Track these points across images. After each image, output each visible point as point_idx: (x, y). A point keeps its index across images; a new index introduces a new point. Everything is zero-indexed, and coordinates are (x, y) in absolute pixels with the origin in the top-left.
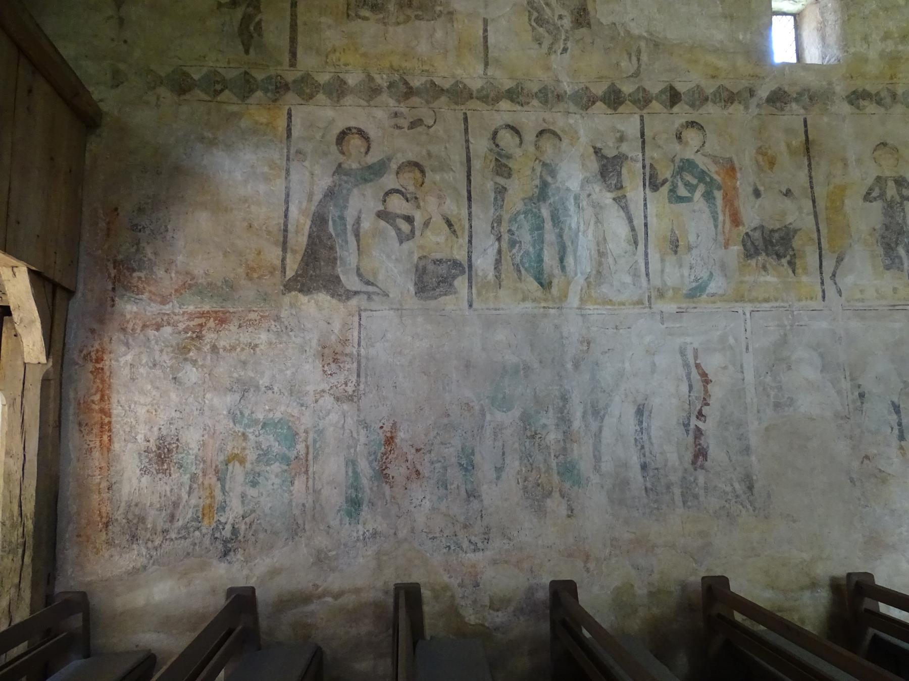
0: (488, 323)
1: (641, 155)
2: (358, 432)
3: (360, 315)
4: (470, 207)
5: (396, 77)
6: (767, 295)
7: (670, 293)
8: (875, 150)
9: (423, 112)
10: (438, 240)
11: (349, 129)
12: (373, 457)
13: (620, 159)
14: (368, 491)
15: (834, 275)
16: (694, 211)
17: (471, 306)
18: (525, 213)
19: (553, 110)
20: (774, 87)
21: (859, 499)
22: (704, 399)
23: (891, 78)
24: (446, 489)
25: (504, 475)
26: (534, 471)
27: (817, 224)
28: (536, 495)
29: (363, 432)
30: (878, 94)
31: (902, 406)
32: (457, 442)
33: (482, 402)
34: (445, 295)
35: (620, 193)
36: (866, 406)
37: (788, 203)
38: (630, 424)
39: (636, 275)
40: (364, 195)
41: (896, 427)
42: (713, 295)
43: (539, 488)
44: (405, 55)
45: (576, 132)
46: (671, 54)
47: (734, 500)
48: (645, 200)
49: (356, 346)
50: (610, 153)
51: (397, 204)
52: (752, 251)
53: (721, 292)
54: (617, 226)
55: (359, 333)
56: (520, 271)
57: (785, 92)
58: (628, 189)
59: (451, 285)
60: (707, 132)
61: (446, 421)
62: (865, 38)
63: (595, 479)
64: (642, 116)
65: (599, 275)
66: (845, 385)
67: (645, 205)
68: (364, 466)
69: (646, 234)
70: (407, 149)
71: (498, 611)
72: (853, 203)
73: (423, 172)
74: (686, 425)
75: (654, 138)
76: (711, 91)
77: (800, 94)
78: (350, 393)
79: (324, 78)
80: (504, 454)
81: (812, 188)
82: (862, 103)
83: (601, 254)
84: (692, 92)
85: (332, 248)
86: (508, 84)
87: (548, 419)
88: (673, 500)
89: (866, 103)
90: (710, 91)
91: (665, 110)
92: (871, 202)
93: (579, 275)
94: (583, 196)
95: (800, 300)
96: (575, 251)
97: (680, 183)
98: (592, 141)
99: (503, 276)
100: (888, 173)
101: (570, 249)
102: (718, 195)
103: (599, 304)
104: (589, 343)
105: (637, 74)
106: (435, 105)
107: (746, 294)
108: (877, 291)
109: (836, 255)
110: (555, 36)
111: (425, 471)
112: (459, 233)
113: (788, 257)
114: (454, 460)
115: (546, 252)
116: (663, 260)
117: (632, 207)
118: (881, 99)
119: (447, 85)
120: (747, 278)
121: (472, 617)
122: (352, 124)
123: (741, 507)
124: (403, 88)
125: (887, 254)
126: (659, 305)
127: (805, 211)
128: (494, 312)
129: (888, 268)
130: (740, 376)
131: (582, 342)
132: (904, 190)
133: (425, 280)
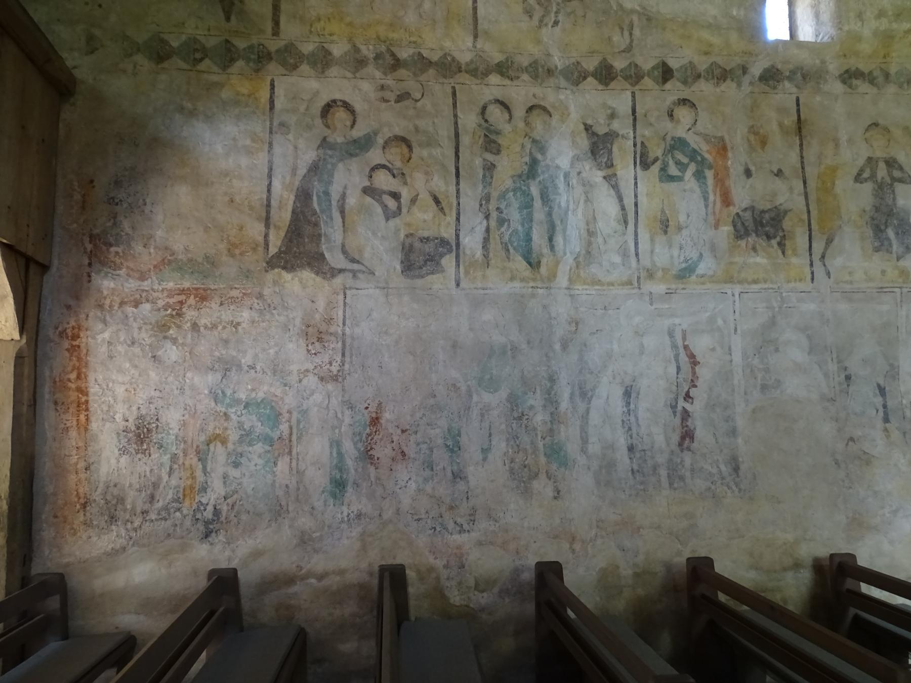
0: (474, 304)
1: (632, 132)
2: (342, 412)
3: (345, 294)
4: (458, 184)
5: (383, 48)
7: (660, 274)
8: (867, 130)
10: (426, 217)
11: (334, 101)
12: (358, 438)
13: (611, 136)
14: (353, 471)
15: (823, 257)
16: (685, 191)
17: (458, 285)
18: (515, 190)
19: (544, 85)
20: (766, 64)
21: (843, 481)
22: (692, 381)
23: (885, 57)
24: (432, 470)
25: (490, 456)
26: (521, 452)
27: (807, 205)
28: (523, 477)
29: (348, 412)
30: (871, 73)
32: (443, 423)
33: (469, 383)
34: (433, 273)
35: (610, 172)
36: (851, 389)
37: (779, 184)
38: (617, 406)
39: (625, 255)
40: (349, 170)
41: (881, 410)
42: (702, 276)
43: (526, 470)
44: (392, 26)
45: (567, 108)
46: (664, 29)
47: (720, 482)
48: (636, 179)
49: (341, 325)
50: (601, 130)
51: (383, 180)
53: (711, 273)
54: (607, 205)
55: (344, 312)
56: (508, 250)
57: (778, 70)
58: (619, 167)
59: (438, 263)
61: (432, 401)
62: (860, 16)
63: (582, 460)
64: (633, 94)
65: (588, 254)
66: (833, 367)
67: (636, 184)
68: (348, 447)
69: (636, 213)
70: (393, 122)
71: (483, 592)
72: (843, 184)
73: (410, 147)
74: (674, 407)
75: (645, 116)
76: (705, 67)
77: (793, 72)
78: (335, 373)
79: (308, 48)
80: (490, 435)
81: (803, 168)
82: (855, 82)
83: (591, 233)
84: (684, 68)
85: (316, 225)
86: (498, 57)
87: (535, 400)
88: (659, 481)
90: (702, 67)
91: (657, 87)
92: (861, 183)
93: (568, 254)
94: (573, 174)
95: (789, 282)
96: (564, 230)
97: (671, 162)
99: (491, 255)
100: (879, 154)
101: (559, 228)
102: (709, 174)
104: (577, 324)
105: (629, 49)
106: (423, 78)
107: (735, 275)
108: (866, 273)
109: (825, 237)
110: (546, 8)
111: (411, 451)
112: (446, 210)
113: (778, 239)
114: (440, 441)
115: (534, 231)
116: (652, 240)
117: (622, 184)
118: (874, 78)
119: (435, 58)
121: (458, 598)
122: (338, 96)
123: (726, 488)
124: (389, 60)
127: (796, 191)
128: (482, 292)
129: (877, 250)
131: (569, 324)
133: (411, 258)
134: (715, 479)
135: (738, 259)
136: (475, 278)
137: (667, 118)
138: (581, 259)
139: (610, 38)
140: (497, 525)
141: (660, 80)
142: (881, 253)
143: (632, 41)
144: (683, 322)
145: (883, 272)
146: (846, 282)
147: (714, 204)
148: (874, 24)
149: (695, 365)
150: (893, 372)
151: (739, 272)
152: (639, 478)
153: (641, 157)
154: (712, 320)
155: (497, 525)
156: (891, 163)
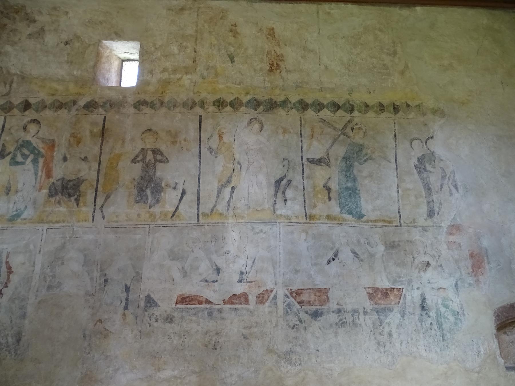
6: (58, 219)
8: (143, 133)
15: (102, 207)
22: (6, 283)
23: (162, 93)
27: (98, 176)
30: (152, 102)
31: (131, 288)
36: (106, 287)
37: (84, 165)
42: (25, 219)
46: (31, 83)
53: (30, 217)
57: (96, 102)
60: (42, 125)
66: (96, 274)
72: (124, 164)
76: (50, 102)
77: (105, 103)
81: (100, 156)
89: (144, 107)
91: (20, 114)
92: (135, 163)
95: (78, 222)
97: (19, 155)
100: (148, 146)
102: (41, 161)
109: (105, 195)
113: (76, 196)
120: (48, 209)
123: (7, 353)
125: (139, 193)
127: (93, 169)
129: (137, 202)
132: (158, 156)
134: (3, 347)
137: (22, 130)
141: (23, 110)
143: (10, 89)
145: (139, 215)
147: (41, 177)
148: (159, 76)
150: (138, 277)
151: (47, 216)
156: (156, 152)
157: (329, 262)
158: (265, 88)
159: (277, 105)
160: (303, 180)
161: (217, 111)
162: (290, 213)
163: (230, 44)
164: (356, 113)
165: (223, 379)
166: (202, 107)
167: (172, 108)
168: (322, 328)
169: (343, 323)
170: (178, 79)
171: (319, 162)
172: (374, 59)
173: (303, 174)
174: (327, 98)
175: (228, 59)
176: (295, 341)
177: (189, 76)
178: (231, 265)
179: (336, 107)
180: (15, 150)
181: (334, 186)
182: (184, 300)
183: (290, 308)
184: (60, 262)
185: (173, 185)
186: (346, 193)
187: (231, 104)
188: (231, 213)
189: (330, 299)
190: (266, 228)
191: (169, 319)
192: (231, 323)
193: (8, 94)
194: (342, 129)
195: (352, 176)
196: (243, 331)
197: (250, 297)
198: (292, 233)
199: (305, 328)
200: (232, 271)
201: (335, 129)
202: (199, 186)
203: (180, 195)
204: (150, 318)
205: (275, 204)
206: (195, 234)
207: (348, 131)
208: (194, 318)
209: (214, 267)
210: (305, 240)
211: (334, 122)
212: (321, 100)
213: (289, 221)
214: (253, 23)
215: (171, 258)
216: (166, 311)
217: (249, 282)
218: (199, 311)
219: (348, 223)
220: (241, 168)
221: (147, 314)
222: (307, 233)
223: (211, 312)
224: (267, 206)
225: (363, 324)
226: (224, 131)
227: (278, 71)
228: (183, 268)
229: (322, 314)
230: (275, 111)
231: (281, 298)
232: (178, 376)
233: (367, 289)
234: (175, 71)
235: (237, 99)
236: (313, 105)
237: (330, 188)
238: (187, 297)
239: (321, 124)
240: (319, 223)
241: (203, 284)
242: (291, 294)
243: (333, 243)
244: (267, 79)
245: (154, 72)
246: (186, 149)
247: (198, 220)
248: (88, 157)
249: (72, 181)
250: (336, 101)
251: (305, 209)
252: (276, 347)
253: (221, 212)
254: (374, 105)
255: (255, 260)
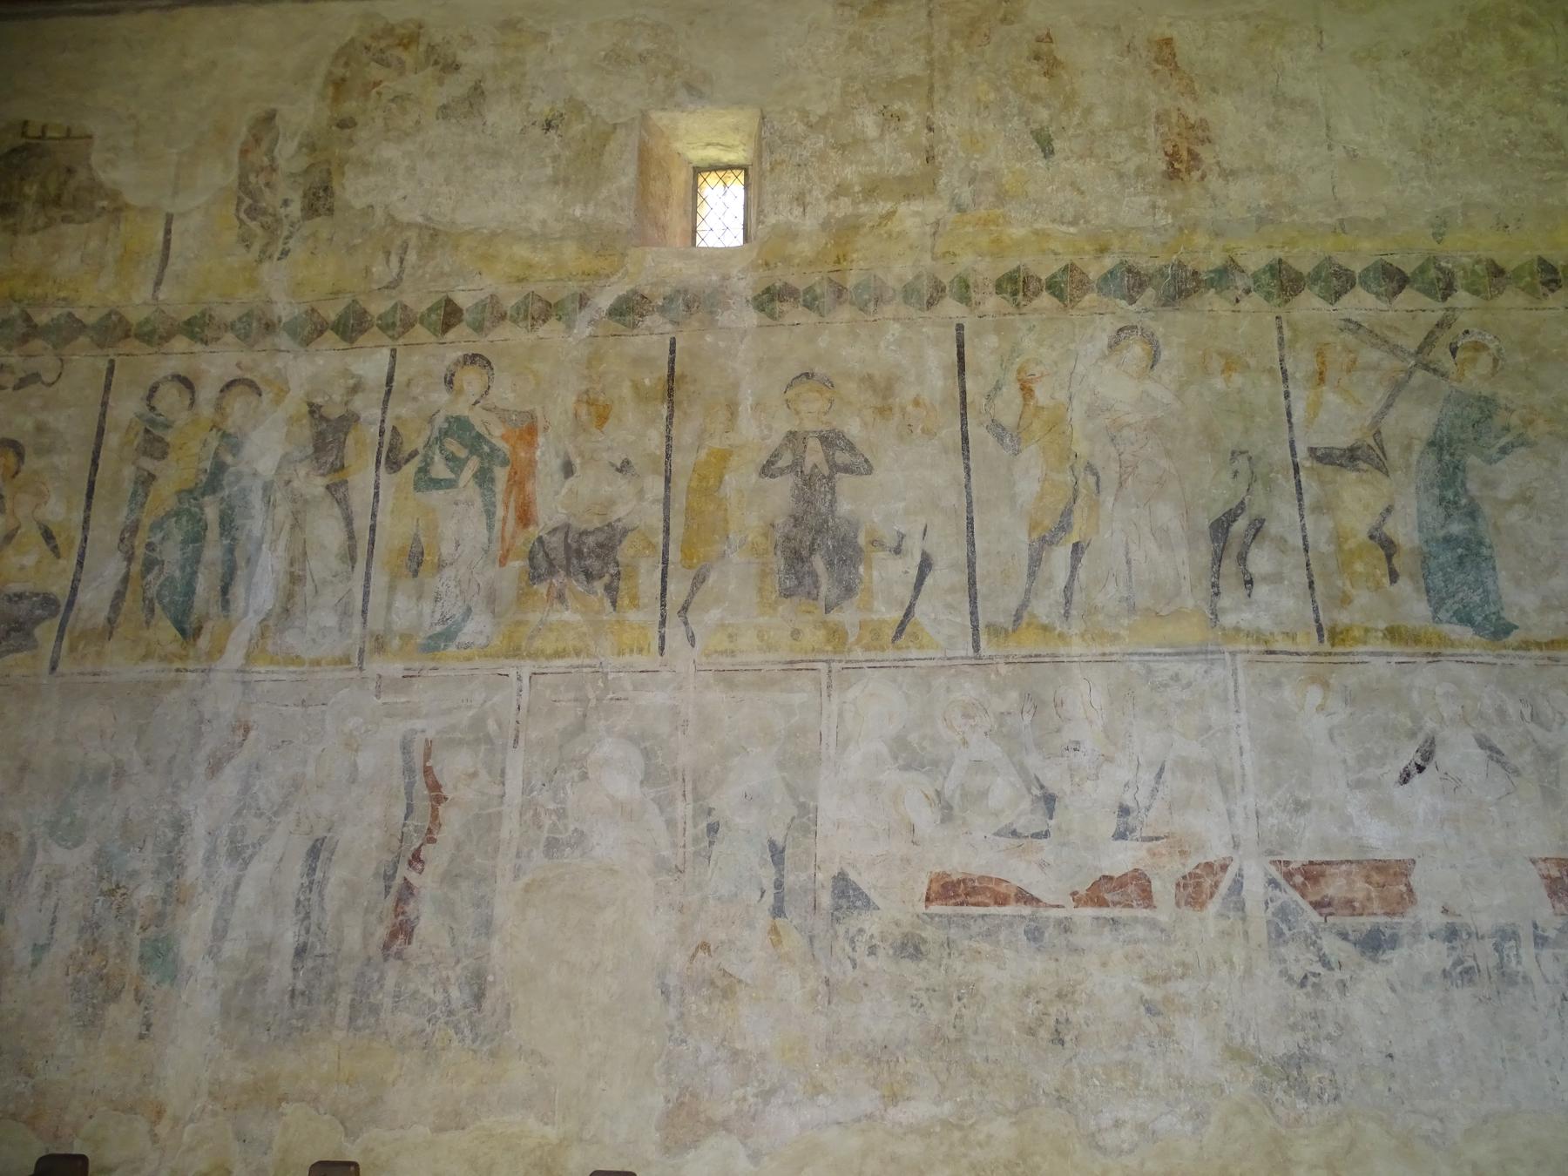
1: (379, 412)
4: (88, 507)
6: (561, 646)
7: (396, 642)
8: (790, 386)
9: (46, 362)
13: (349, 421)
15: (685, 608)
17: (53, 668)
21: (671, 1028)
22: (430, 831)
23: (838, 261)
27: (667, 520)
30: (810, 289)
34: (17, 650)
35: (336, 478)
36: (716, 849)
37: (623, 485)
39: (345, 614)
44: (34, 278)
45: (286, 382)
48: (377, 487)
50: (334, 412)
52: (544, 566)
53: (482, 641)
54: (327, 532)
56: (152, 611)
59: (29, 635)
63: (205, 969)
64: (394, 351)
65: (286, 610)
66: (683, 809)
67: (376, 495)
72: (739, 479)
73: (20, 456)
74: (388, 878)
75: (408, 385)
77: (669, 299)
80: (53, 923)
81: (668, 456)
84: (481, 307)
87: (143, 861)
88: (332, 1015)
89: (785, 307)
90: (509, 304)
91: (433, 339)
92: (773, 476)
93: (251, 614)
95: (620, 653)
96: (251, 575)
98: (307, 395)
99: (121, 619)
100: (809, 425)
101: (241, 573)
102: (501, 474)
103: (278, 663)
104: (247, 730)
108: (760, 637)
109: (692, 573)
112: (62, 549)
113: (607, 579)
116: (392, 588)
119: (91, 319)
123: (451, 1032)
124: (21, 328)
125: (790, 566)
126: (375, 666)
127: (649, 496)
129: (787, 594)
130: (497, 790)
132: (838, 454)
135: (534, 617)
136: (84, 656)
138: (271, 623)
139: (367, 270)
140: (31, 1082)
142: (795, 599)
144: (428, 727)
145: (796, 634)
146: (723, 653)
149: (439, 803)
150: (805, 819)
151: (531, 638)
152: (300, 1005)
153: (390, 450)
154: (478, 723)
155: (31, 1082)
156: (830, 440)
157: (1406, 778)
158: (1155, 230)
159: (1199, 282)
160: (1302, 517)
161: (1011, 310)
162: (1265, 623)
163: (1036, 98)
164: (1462, 298)
165: (1093, 1135)
166: (964, 298)
167: (871, 306)
168: (1398, 987)
169: (1468, 971)
170: (881, 217)
171: (1351, 457)
172: (1513, 119)
173: (1300, 500)
174: (1361, 254)
175: (1034, 145)
176: (1313, 1023)
177: (916, 206)
178: (1089, 785)
179: (1393, 279)
180: (428, 445)
181: (1404, 531)
182: (949, 890)
183: (1287, 921)
184: (575, 773)
185: (891, 542)
186: (1447, 557)
187: (1053, 287)
188: (1076, 627)
189: (1418, 894)
190: (1192, 670)
191: (911, 948)
192: (1104, 964)
193: (395, 284)
194: (1420, 350)
195: (1464, 501)
196: (1143, 988)
197: (1156, 885)
198: (1277, 684)
199: (1343, 986)
200: (1090, 803)
201: (1394, 350)
202: (971, 543)
203: (914, 572)
204: (852, 941)
205: (1217, 594)
206: (968, 689)
207: (1440, 355)
208: (986, 947)
209: (1036, 792)
210: (1321, 708)
211: (1389, 328)
212: (1342, 260)
213: (1263, 648)
214: (1105, 28)
215: (901, 762)
216: (897, 924)
217: (1151, 839)
218: (999, 926)
219: (1462, 651)
220: (1097, 484)
221: (841, 929)
222: (1326, 685)
223: (1037, 928)
224: (1190, 603)
225: (1535, 976)
226: (1037, 370)
227: (1196, 174)
228: (938, 793)
229: (1394, 942)
230: (1194, 301)
231: (1255, 888)
232: (953, 1120)
233: (1542, 865)
234: (872, 190)
235: (1069, 269)
236: (1316, 277)
237: (1392, 542)
238: (959, 882)
239: (1349, 338)
240: (1366, 653)
241: (1005, 842)
242: (1289, 876)
243: (1416, 718)
244: (1161, 202)
245: (808, 199)
246: (923, 431)
247: (976, 647)
248: (631, 459)
249: (592, 533)
250: (1395, 260)
251: (1316, 610)
252: (1252, 1041)
253: (1045, 620)
254: (1521, 268)
255: (1162, 769)
